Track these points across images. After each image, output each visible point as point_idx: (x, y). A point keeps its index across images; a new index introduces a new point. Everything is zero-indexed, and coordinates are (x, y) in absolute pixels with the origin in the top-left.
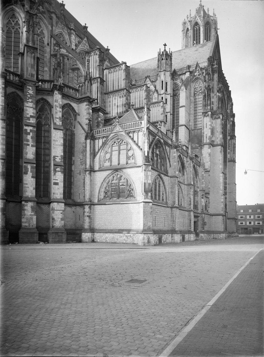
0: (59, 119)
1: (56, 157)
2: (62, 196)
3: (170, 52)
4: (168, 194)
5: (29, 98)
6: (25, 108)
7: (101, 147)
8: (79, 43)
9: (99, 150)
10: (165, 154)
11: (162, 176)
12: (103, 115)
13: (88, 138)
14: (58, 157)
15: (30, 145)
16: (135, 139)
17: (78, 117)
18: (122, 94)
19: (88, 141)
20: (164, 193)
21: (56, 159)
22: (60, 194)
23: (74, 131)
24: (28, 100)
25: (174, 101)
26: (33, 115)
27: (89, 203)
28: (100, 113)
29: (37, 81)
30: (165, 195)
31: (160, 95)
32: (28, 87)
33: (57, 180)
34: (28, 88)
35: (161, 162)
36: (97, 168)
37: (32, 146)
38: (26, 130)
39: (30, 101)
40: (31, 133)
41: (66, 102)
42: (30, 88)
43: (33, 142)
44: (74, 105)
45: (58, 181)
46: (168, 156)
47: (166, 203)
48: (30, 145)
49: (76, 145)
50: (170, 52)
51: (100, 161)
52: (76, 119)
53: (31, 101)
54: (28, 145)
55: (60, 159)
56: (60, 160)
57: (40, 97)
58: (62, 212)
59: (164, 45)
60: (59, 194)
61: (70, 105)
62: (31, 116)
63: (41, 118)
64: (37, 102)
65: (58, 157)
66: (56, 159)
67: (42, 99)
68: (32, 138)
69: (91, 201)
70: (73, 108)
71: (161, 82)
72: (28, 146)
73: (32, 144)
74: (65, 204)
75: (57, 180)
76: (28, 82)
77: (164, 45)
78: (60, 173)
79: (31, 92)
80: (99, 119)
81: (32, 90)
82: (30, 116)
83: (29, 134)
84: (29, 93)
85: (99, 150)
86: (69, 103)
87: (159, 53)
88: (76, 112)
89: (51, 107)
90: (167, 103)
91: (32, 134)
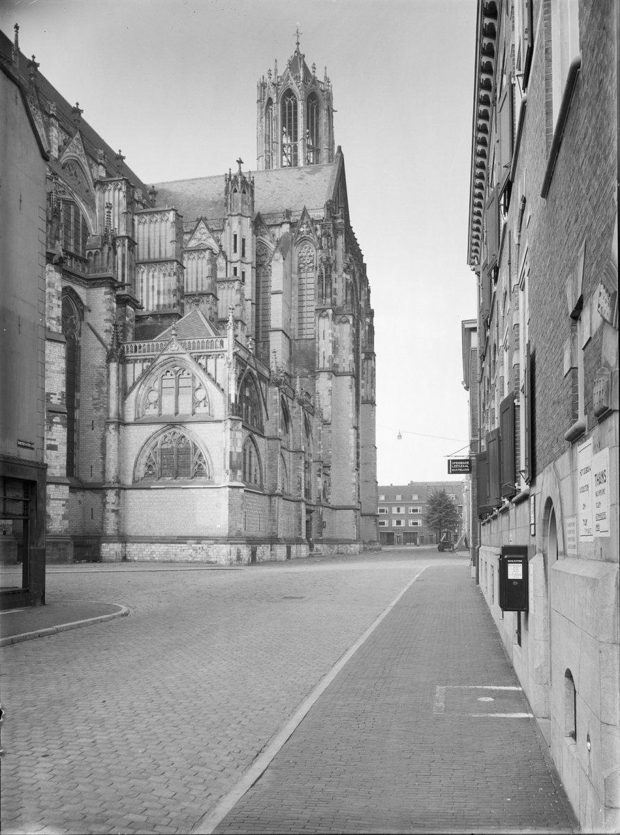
1: (51, 396)
2: (64, 472)
3: (250, 178)
4: (264, 470)
7: (139, 379)
8: (65, 144)
9: (134, 384)
10: (258, 396)
11: (255, 436)
12: (132, 310)
13: (113, 359)
14: (55, 394)
16: (211, 369)
17: (87, 314)
18: (169, 270)
19: (113, 366)
20: (258, 468)
21: (52, 398)
22: (61, 468)
23: (78, 342)
25: (258, 276)
27: (117, 485)
28: (128, 307)
30: (258, 471)
31: (231, 262)
33: (55, 440)
35: (252, 411)
36: (130, 417)
41: (67, 284)
44: (80, 290)
45: (56, 443)
46: (264, 399)
47: (261, 487)
49: (82, 370)
50: (250, 178)
51: (137, 405)
52: (83, 317)
55: (59, 399)
56: (60, 401)
58: (64, 503)
59: (237, 161)
60: (58, 467)
61: (72, 291)
65: (55, 394)
66: (52, 398)
69: (119, 482)
70: (77, 297)
71: (233, 236)
74: (70, 488)
75: (55, 440)
77: (237, 161)
78: (60, 426)
80: (127, 319)
85: (134, 384)
86: (70, 287)
87: (228, 177)
88: (82, 304)
90: (246, 280)
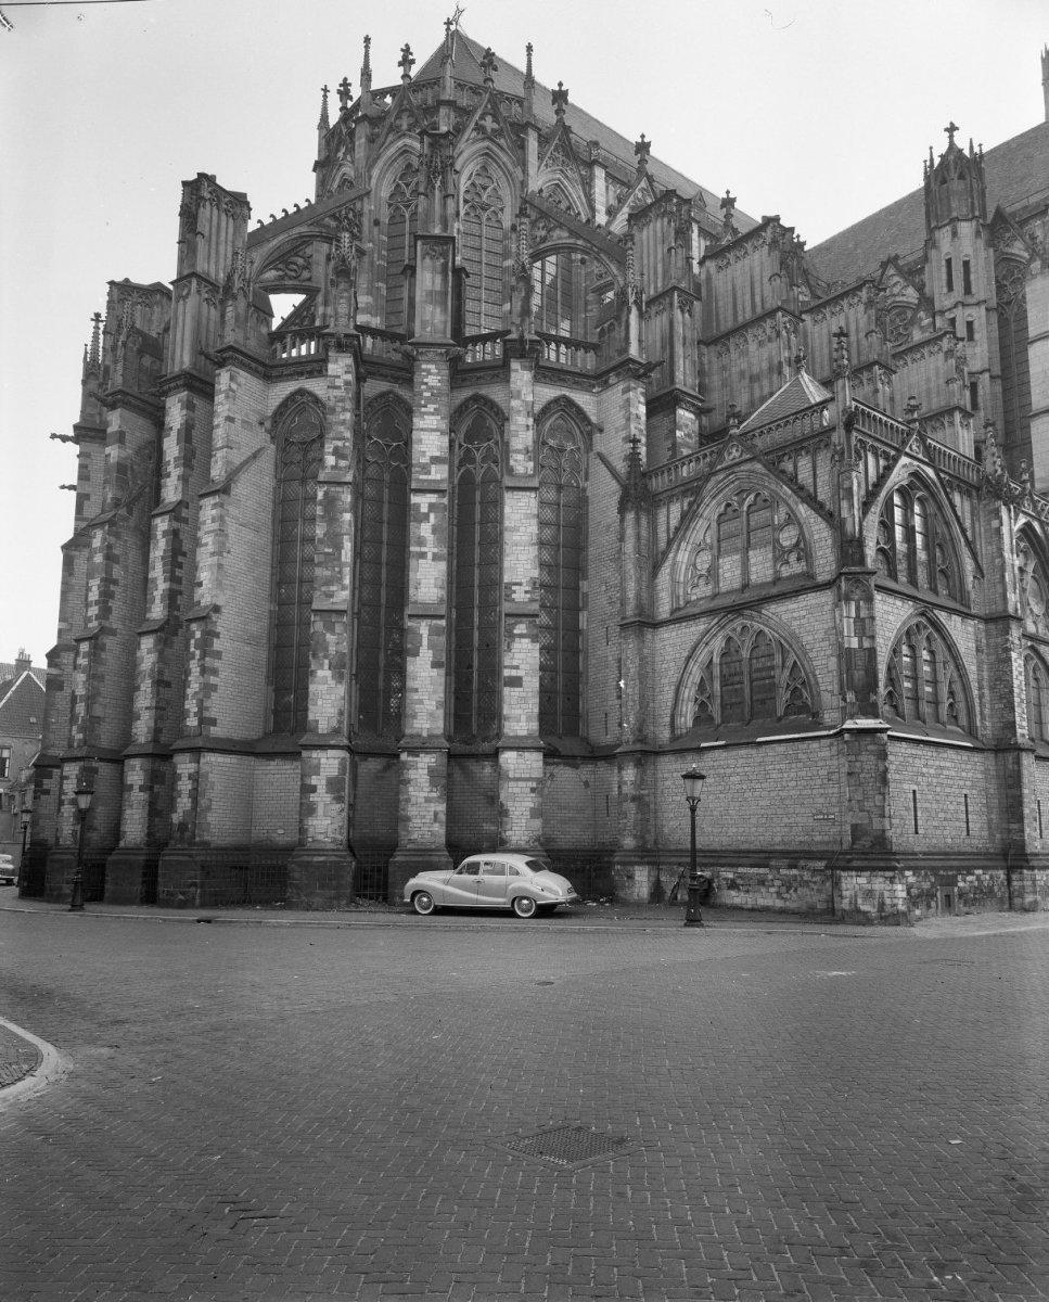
0: (524, 452)
1: (514, 588)
2: (535, 725)
3: (971, 148)
4: (975, 692)
5: (428, 400)
6: (415, 435)
7: (677, 529)
8: (619, 202)
9: (670, 542)
10: (947, 524)
11: (942, 616)
12: (692, 416)
13: (630, 505)
14: (520, 584)
15: (430, 556)
16: (804, 475)
17: (597, 436)
18: (768, 331)
19: (630, 516)
20: (957, 687)
21: (515, 592)
22: (529, 719)
23: (584, 490)
24: (423, 409)
25: (1003, 323)
26: (438, 454)
27: (638, 747)
28: (680, 412)
29: (452, 342)
30: (960, 696)
31: (942, 313)
32: (424, 366)
33: (517, 668)
34: (424, 371)
35: (931, 559)
36: (664, 610)
37: (436, 557)
38: (418, 506)
39: (432, 410)
40: (432, 516)
41: (549, 393)
42: (432, 367)
43: (439, 542)
44: (582, 399)
45: (520, 673)
46: (964, 531)
47: (971, 732)
48: (430, 556)
49: (592, 538)
50: (971, 148)
51: (674, 582)
52: (591, 445)
53: (435, 409)
54: (423, 555)
55: (526, 592)
56: (528, 596)
57: (466, 393)
58: (534, 785)
59: (946, 130)
60: (523, 718)
61: (570, 403)
62: (435, 460)
63: (473, 461)
64: (455, 417)
65: (520, 584)
66: (515, 592)
67: (476, 398)
68: (435, 530)
69: (642, 739)
70: (580, 411)
71: (944, 263)
72: (421, 561)
73: (436, 550)
74: (545, 756)
75: (517, 668)
76: (424, 350)
77: (946, 130)
78: (527, 640)
79: (433, 381)
80: (678, 433)
81: (438, 374)
82: (432, 458)
83: (426, 517)
84: (426, 384)
85: (670, 542)
86: (564, 397)
87: (928, 163)
88: (589, 423)
89: (502, 418)
90: (977, 336)
91: (436, 518)
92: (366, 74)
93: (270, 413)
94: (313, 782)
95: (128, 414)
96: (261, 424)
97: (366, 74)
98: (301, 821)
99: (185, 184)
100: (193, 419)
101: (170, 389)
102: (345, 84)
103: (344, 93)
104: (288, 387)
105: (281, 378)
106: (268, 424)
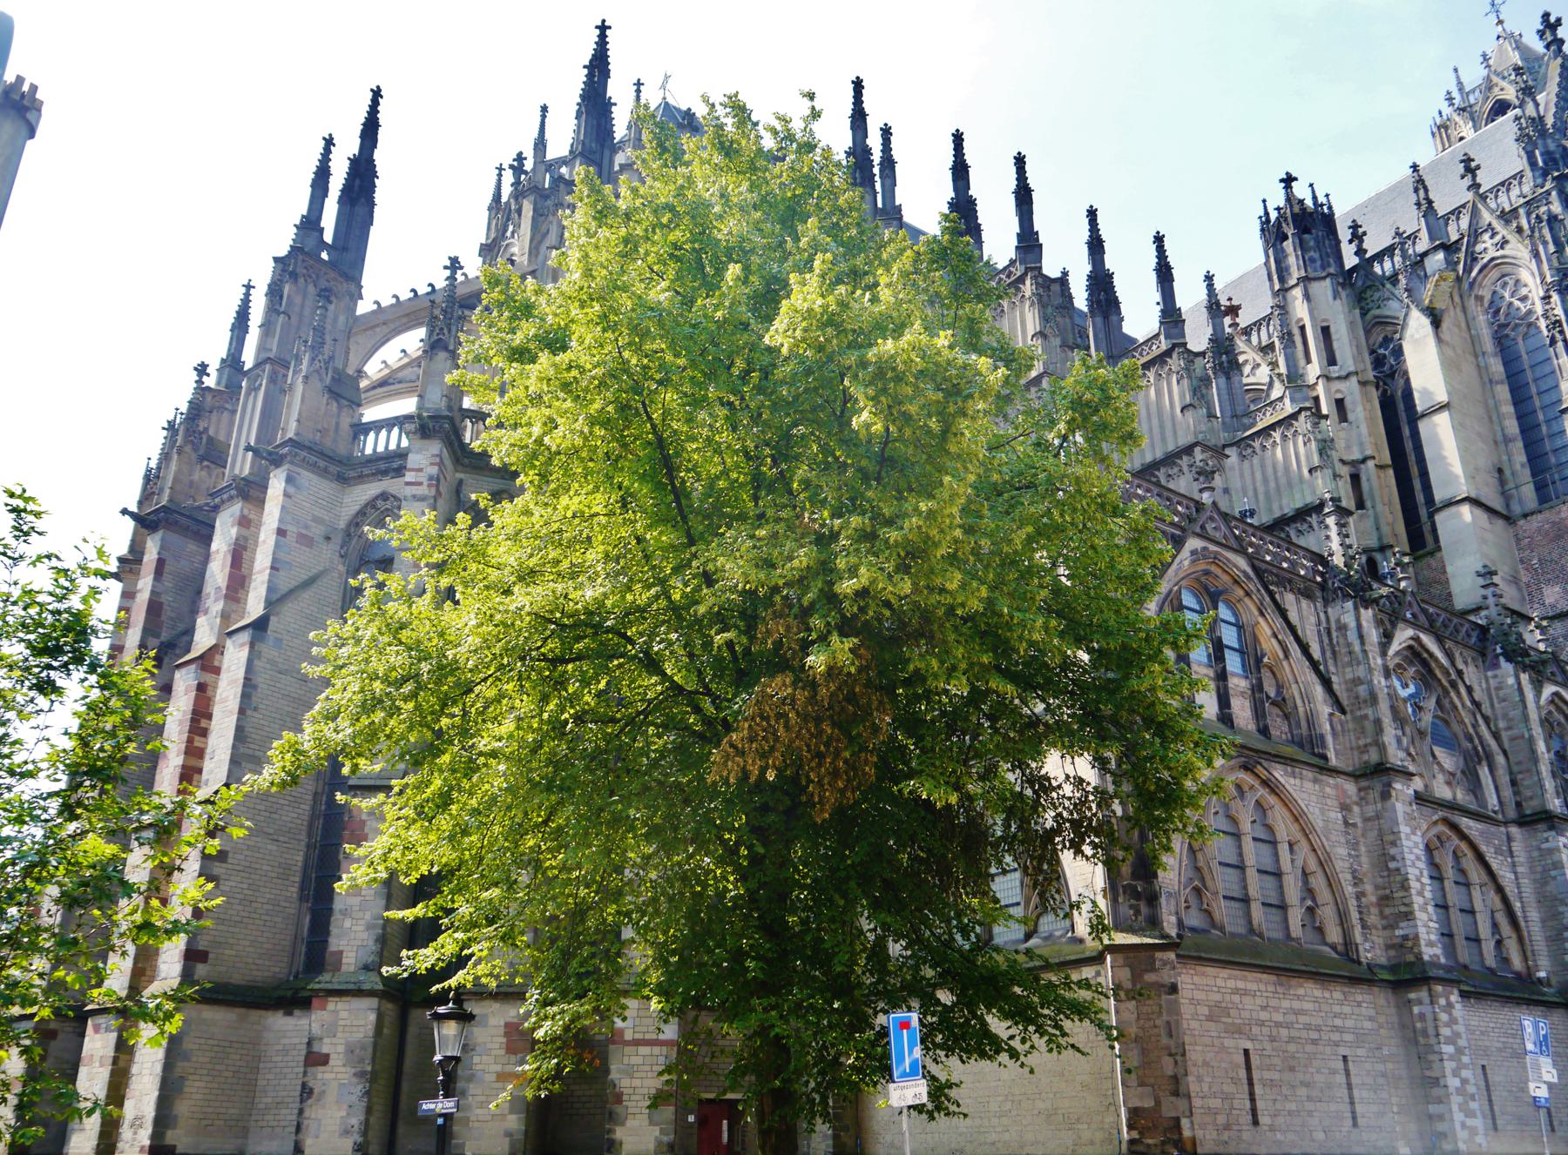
92: (540, 144)
93: (342, 525)
94: (325, 1050)
95: (174, 538)
96: (328, 538)
97: (540, 144)
98: (301, 1112)
99: (276, 260)
100: (246, 539)
101: (223, 502)
102: (520, 158)
103: (518, 169)
104: (371, 490)
105: (361, 479)
106: (338, 539)
